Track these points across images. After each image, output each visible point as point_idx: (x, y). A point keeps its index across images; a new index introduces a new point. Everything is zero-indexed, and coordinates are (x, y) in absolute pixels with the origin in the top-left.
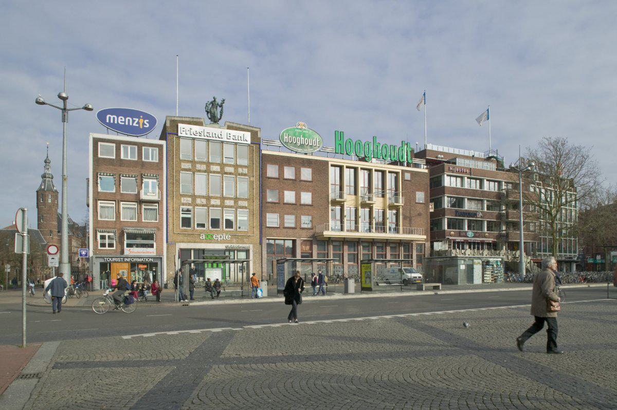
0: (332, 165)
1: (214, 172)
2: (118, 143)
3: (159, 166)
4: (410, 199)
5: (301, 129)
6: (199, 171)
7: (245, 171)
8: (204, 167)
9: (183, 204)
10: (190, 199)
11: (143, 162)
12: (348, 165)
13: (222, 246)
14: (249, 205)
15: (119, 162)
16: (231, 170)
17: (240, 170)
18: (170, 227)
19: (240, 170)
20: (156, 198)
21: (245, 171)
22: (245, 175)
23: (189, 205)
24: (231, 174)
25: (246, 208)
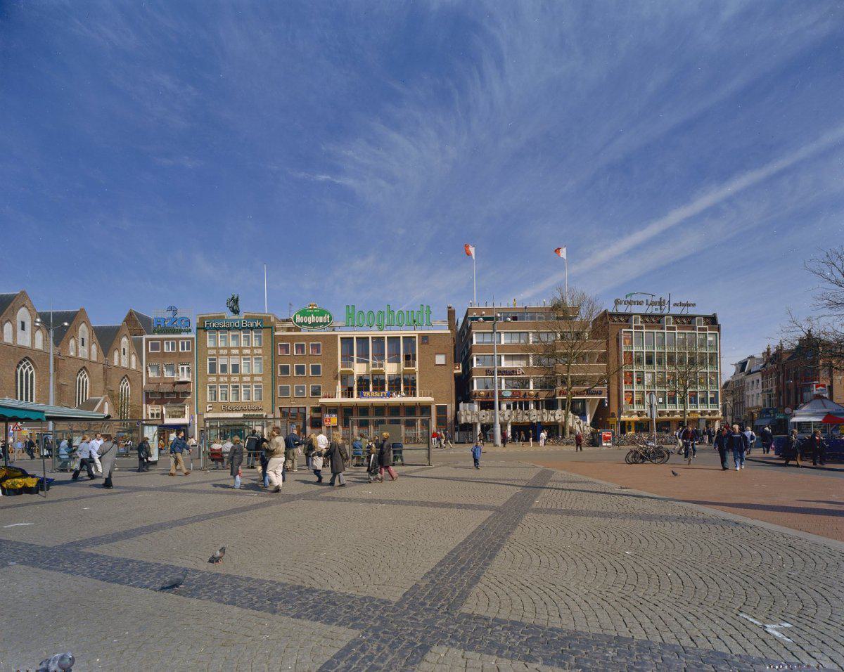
0: (341, 338)
1: (234, 355)
2: (162, 340)
3: (191, 354)
4: (428, 364)
5: (312, 309)
6: (222, 355)
7: (260, 351)
8: (225, 352)
9: (210, 383)
10: (215, 378)
11: (180, 353)
12: (357, 336)
13: (240, 415)
14: (263, 380)
15: (165, 355)
16: (248, 351)
17: (255, 351)
18: (200, 401)
19: (255, 351)
20: (189, 380)
21: (260, 351)
22: (260, 355)
23: (214, 383)
24: (247, 355)
25: (260, 382)
